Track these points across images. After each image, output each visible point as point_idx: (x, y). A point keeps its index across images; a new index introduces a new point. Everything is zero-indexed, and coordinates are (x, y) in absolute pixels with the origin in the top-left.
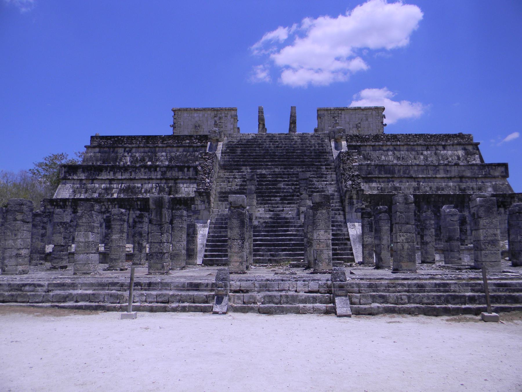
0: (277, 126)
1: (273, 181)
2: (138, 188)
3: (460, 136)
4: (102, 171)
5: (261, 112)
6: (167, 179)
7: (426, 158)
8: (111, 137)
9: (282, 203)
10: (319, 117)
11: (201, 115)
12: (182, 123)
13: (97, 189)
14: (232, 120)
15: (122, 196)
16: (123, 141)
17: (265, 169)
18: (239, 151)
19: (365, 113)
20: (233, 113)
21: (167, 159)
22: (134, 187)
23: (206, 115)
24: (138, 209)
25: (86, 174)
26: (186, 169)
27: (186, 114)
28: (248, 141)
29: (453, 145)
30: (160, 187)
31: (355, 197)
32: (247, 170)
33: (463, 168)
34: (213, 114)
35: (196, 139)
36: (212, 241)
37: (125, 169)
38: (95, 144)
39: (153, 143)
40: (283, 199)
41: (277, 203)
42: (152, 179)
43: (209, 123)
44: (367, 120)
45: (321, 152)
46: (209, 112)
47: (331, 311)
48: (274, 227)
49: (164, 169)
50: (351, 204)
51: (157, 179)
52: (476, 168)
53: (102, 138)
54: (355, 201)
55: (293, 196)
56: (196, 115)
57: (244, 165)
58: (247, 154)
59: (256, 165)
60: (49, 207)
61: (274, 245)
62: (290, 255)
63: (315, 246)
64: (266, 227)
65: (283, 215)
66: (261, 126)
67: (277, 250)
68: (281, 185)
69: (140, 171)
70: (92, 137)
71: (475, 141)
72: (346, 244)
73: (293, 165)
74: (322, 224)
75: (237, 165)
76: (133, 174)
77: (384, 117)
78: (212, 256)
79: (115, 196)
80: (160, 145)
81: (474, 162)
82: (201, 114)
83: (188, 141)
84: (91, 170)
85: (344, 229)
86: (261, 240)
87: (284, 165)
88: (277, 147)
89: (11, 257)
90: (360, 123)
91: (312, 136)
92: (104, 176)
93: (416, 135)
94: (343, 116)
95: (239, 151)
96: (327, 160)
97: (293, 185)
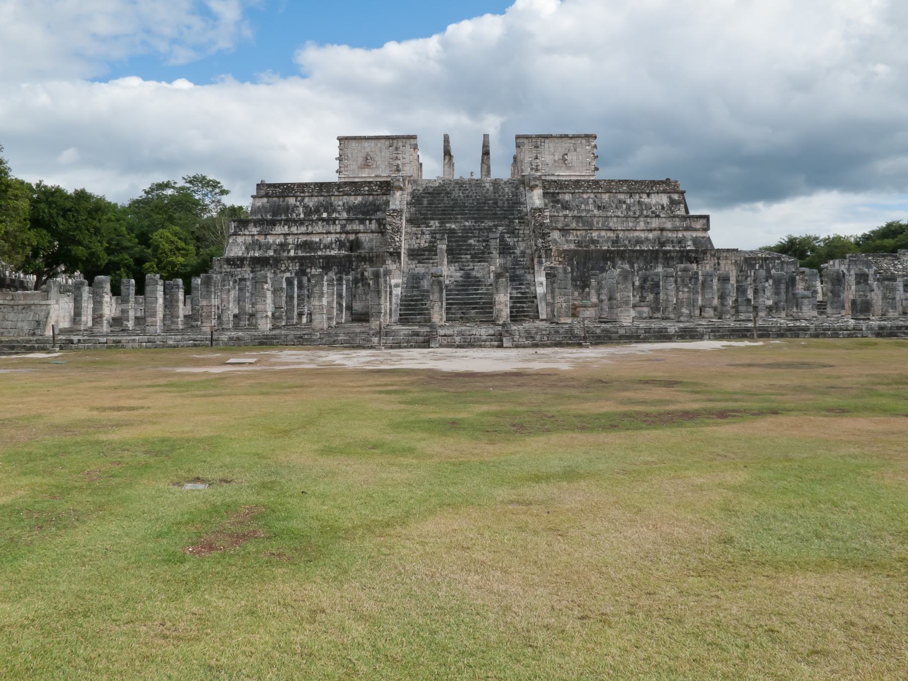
0: (467, 167)
1: (463, 237)
2: (316, 243)
3: (667, 182)
4: (275, 225)
5: (446, 140)
6: (347, 233)
7: (628, 208)
8: (280, 185)
9: (473, 262)
10: (518, 146)
11: (373, 145)
12: (350, 155)
13: (271, 245)
15: (300, 254)
16: (293, 189)
17: (455, 223)
18: (425, 202)
19: (573, 141)
21: (344, 209)
22: (312, 242)
23: (379, 145)
24: (320, 268)
25: (258, 229)
26: (368, 222)
27: (354, 144)
28: (435, 189)
29: (658, 193)
30: (340, 241)
32: (435, 224)
33: (664, 220)
34: (388, 143)
35: (376, 185)
36: (406, 301)
37: (301, 222)
38: (263, 192)
39: (327, 192)
40: (474, 257)
41: (467, 262)
42: (330, 233)
43: (383, 154)
44: (575, 150)
45: (515, 203)
46: (383, 141)
47: (501, 346)
48: (464, 286)
49: (344, 222)
50: (540, 263)
51: (337, 233)
52: (677, 220)
53: (270, 185)
54: (544, 260)
55: (483, 253)
57: (432, 219)
58: (434, 203)
59: (444, 219)
60: (225, 266)
61: (465, 304)
62: (480, 313)
63: (498, 307)
64: (457, 286)
65: (474, 273)
66: (447, 157)
67: (468, 309)
68: (472, 241)
69: (317, 224)
70: (258, 185)
71: (681, 189)
72: (533, 302)
73: (484, 218)
74: (502, 289)
75: (425, 218)
76: (310, 227)
77: (595, 147)
78: (406, 314)
79: (292, 253)
80: (336, 193)
81: (678, 213)
82: (372, 143)
83: (367, 188)
84: (263, 224)
85: (533, 288)
86: (453, 299)
87: (475, 218)
88: (467, 196)
89: (262, 318)
91: (505, 183)
92: (279, 229)
93: (619, 181)
94: (546, 145)
95: (425, 202)
96: (520, 212)
97: (484, 241)
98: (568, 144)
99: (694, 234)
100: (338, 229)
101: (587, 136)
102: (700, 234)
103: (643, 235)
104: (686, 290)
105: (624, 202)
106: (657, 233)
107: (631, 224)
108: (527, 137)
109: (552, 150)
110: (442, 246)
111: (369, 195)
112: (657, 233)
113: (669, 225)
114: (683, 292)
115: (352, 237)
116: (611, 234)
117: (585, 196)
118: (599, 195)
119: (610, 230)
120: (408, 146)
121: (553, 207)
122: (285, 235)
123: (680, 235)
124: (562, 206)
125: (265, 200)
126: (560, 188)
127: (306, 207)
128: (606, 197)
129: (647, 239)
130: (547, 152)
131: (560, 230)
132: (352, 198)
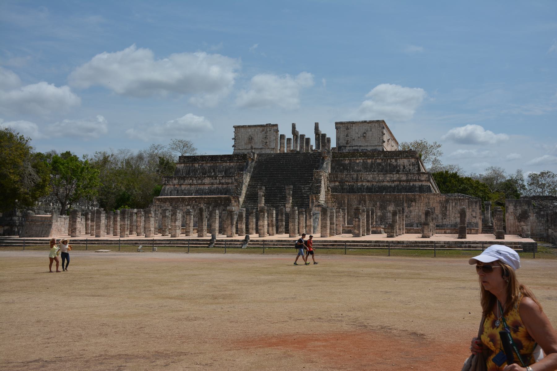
6: (223, 184)
10: (337, 128)
19: (370, 125)
20: (275, 128)
23: (256, 130)
27: (242, 130)
30: (218, 189)
31: (314, 198)
34: (261, 129)
44: (371, 130)
46: (259, 128)
50: (313, 202)
56: (249, 130)
66: (295, 137)
82: (253, 129)
90: (365, 133)
94: (354, 128)
98: (366, 127)
99: (420, 184)
101: (378, 121)
102: (424, 183)
103: (388, 184)
104: (357, 220)
106: (396, 183)
107: (381, 178)
108: (341, 123)
109: (357, 131)
110: (261, 193)
111: (237, 162)
112: (396, 183)
113: (404, 178)
114: (356, 221)
115: (225, 186)
117: (357, 161)
118: (365, 160)
119: (368, 181)
120: (272, 131)
121: (338, 168)
122: (190, 185)
123: (411, 184)
124: (343, 167)
125: (183, 165)
126: (344, 157)
128: (369, 161)
129: (391, 187)
132: (228, 164)
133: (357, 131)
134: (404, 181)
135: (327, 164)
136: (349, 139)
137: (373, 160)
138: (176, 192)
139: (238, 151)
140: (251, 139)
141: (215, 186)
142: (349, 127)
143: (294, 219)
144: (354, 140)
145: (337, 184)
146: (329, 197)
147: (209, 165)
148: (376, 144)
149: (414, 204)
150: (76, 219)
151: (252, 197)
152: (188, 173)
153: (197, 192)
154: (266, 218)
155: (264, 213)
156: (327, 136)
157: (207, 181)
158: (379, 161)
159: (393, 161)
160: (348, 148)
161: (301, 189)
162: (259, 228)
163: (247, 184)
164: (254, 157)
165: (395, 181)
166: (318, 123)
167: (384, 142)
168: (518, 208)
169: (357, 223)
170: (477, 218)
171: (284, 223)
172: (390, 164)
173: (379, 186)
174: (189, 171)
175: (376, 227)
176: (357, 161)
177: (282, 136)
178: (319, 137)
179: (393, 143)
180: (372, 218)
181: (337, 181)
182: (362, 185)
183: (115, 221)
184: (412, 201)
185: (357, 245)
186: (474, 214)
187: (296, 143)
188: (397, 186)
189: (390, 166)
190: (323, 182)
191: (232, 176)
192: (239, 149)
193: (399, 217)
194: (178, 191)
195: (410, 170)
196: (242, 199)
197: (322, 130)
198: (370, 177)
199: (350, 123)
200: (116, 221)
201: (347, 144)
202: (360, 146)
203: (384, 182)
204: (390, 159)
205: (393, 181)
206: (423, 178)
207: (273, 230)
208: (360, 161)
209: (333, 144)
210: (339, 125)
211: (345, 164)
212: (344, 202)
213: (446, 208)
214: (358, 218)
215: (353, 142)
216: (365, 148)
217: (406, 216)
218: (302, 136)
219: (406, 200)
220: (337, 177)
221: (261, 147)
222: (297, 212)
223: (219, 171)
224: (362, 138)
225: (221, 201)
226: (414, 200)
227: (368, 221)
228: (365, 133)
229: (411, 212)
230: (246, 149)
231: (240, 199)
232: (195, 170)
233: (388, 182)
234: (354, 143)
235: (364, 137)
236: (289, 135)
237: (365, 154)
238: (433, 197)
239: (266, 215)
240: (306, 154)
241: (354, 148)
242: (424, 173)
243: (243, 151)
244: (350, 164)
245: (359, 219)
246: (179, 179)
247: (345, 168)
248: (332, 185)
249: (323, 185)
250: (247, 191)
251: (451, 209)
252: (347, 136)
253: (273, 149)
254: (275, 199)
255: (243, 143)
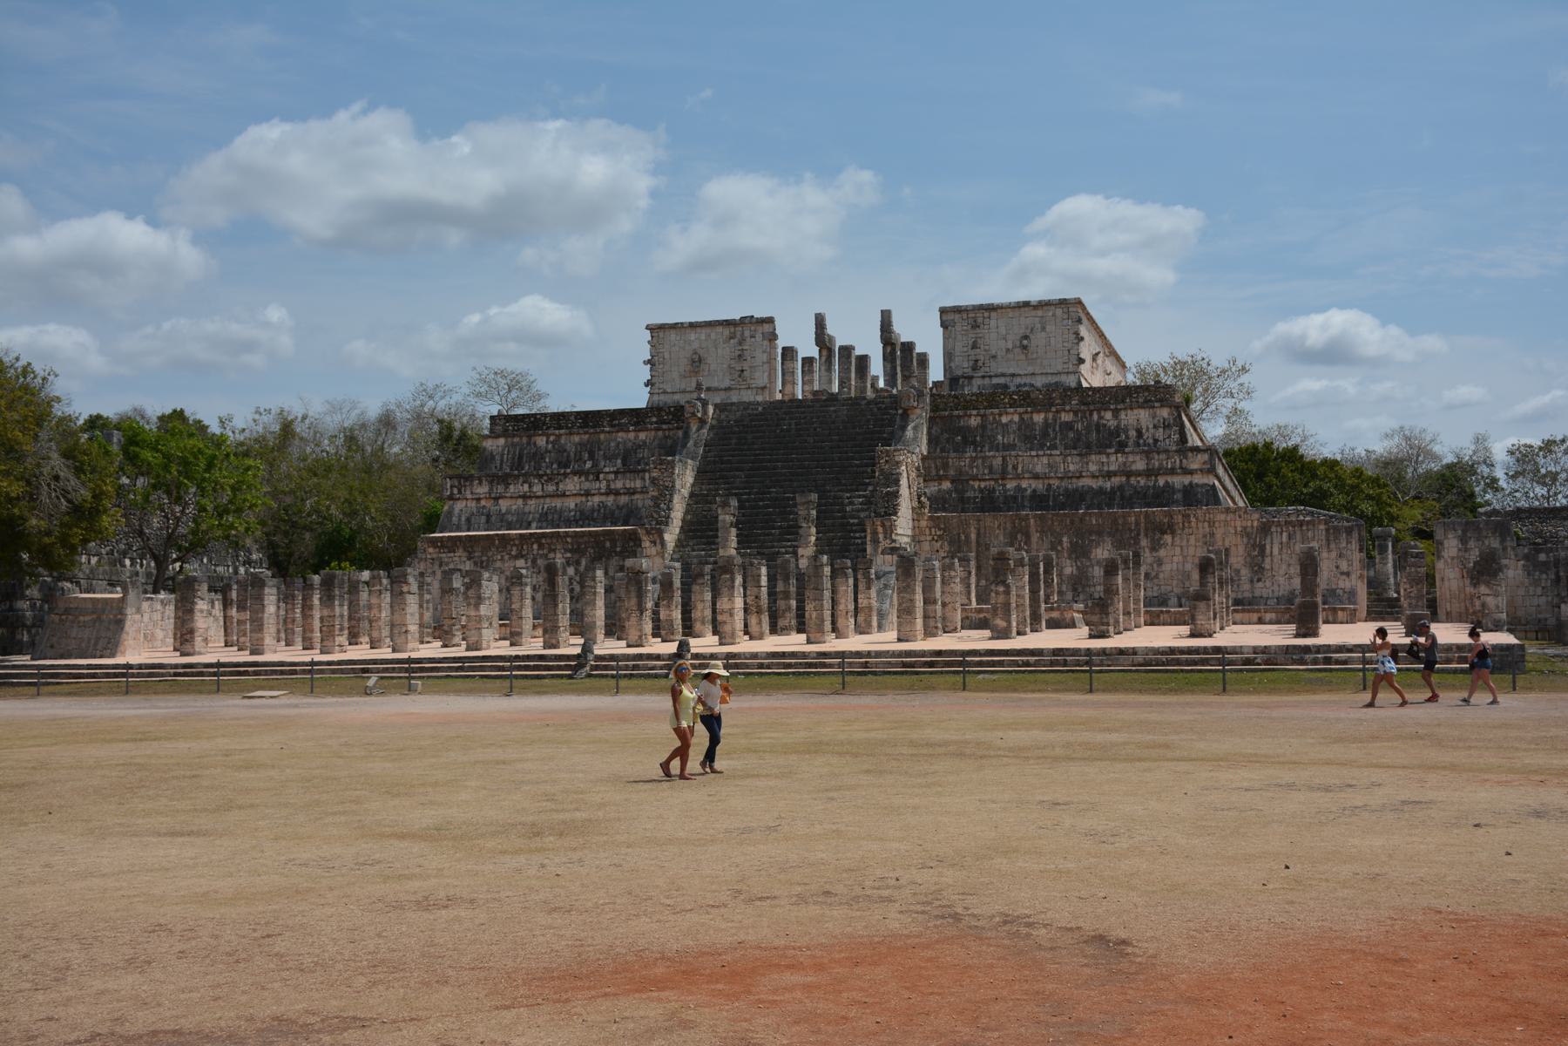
6: (617, 493)
10: (944, 325)
12: (667, 356)
14: (766, 343)
19: (1040, 313)
20: (766, 327)
23: (713, 336)
30: (605, 507)
31: (880, 529)
34: (727, 332)
39: (594, 427)
44: (1043, 329)
46: (720, 329)
50: (876, 541)
54: (881, 536)
66: (825, 353)
82: (704, 331)
90: (1026, 337)
94: (993, 323)
98: (1029, 319)
99: (1187, 480)
100: (603, 485)
101: (1063, 302)
102: (1198, 479)
103: (1094, 484)
104: (1001, 589)
105: (1071, 428)
106: (1116, 481)
108: (957, 310)
109: (1003, 330)
111: (657, 430)
112: (1116, 481)
113: (1140, 464)
114: (997, 593)
115: (623, 499)
116: (1035, 484)
117: (1004, 419)
118: (1026, 417)
119: (1036, 477)
120: (759, 337)
121: (948, 441)
122: (525, 497)
123: (1161, 482)
124: (964, 438)
125: (502, 441)
126: (965, 408)
127: (562, 450)
128: (1039, 418)
129: (1101, 491)
130: (994, 336)
131: (953, 482)
132: (632, 435)
133: (1003, 330)
134: (1138, 474)
135: (915, 428)
136: (980, 354)
137: (1050, 415)
138: (483, 519)
139: (662, 397)
140: (697, 362)
141: (597, 499)
142: (980, 320)
143: (819, 589)
144: (994, 357)
145: (946, 485)
146: (924, 523)
147: (576, 439)
148: (1060, 368)
149: (1168, 538)
150: (193, 603)
151: (700, 530)
152: (518, 464)
153: (544, 518)
154: (739, 591)
155: (732, 574)
156: (918, 350)
157: (572, 485)
158: (1066, 417)
159: (1108, 415)
160: (977, 382)
161: (842, 504)
162: (719, 618)
163: (686, 492)
164: (705, 412)
165: (1115, 474)
166: (889, 312)
167: (1081, 361)
168: (1472, 544)
169: (1001, 599)
170: (1353, 577)
171: (793, 603)
172: (1098, 425)
173: (1066, 489)
174: (520, 457)
175: (1058, 609)
176: (1004, 419)
177: (789, 353)
178: (893, 351)
179: (1110, 365)
180: (1048, 584)
181: (946, 477)
182: (1019, 488)
183: (307, 607)
184: (1163, 533)
185: (1001, 663)
186: (1344, 566)
187: (829, 369)
188: (1121, 488)
189: (1098, 431)
190: (904, 482)
191: (644, 471)
192: (665, 392)
193: (1126, 579)
194: (488, 516)
195: (1156, 441)
196: (671, 536)
197: (903, 332)
198: (1040, 466)
199: (981, 308)
200: (311, 608)
201: (975, 368)
202: (1013, 375)
203: (1081, 477)
204: (1099, 411)
205: (1109, 475)
206: (1196, 462)
207: (760, 623)
208: (1010, 417)
209: (936, 373)
210: (950, 316)
211: (968, 428)
212: (968, 537)
213: (1262, 549)
214: (1004, 582)
215: (993, 364)
216: (1028, 380)
217: (1147, 575)
218: (846, 351)
219: (1146, 530)
220: (945, 466)
221: (727, 383)
222: (827, 570)
223: (605, 458)
224: (1018, 350)
225: (614, 542)
226: (1170, 529)
227: (1034, 592)
228: (1026, 337)
229: (1160, 562)
230: (684, 392)
231: (667, 537)
232: (537, 456)
233: (1094, 476)
234: (995, 368)
235: (1025, 347)
236: (808, 348)
237: (1026, 399)
238: (1223, 517)
239: (739, 580)
240: (854, 403)
241: (995, 381)
242: (1196, 450)
243: (677, 397)
244: (983, 427)
245: (1008, 587)
246: (491, 483)
247: (968, 439)
248: (933, 488)
249: (904, 491)
250: (686, 513)
251: (1276, 551)
252: (974, 346)
253: (763, 388)
254: (766, 533)
255: (675, 375)
